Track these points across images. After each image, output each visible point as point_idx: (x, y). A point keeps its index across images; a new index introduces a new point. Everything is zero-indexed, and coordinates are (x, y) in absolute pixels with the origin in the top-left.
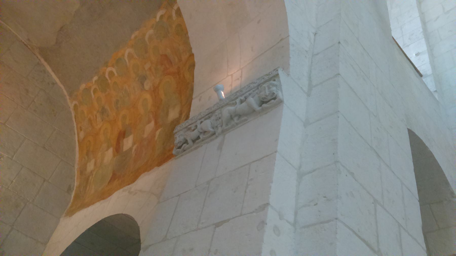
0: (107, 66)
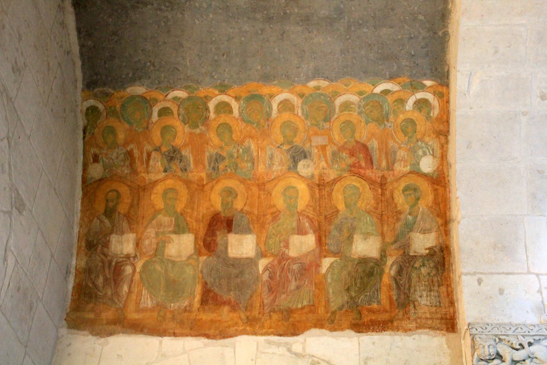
0: (222, 92)
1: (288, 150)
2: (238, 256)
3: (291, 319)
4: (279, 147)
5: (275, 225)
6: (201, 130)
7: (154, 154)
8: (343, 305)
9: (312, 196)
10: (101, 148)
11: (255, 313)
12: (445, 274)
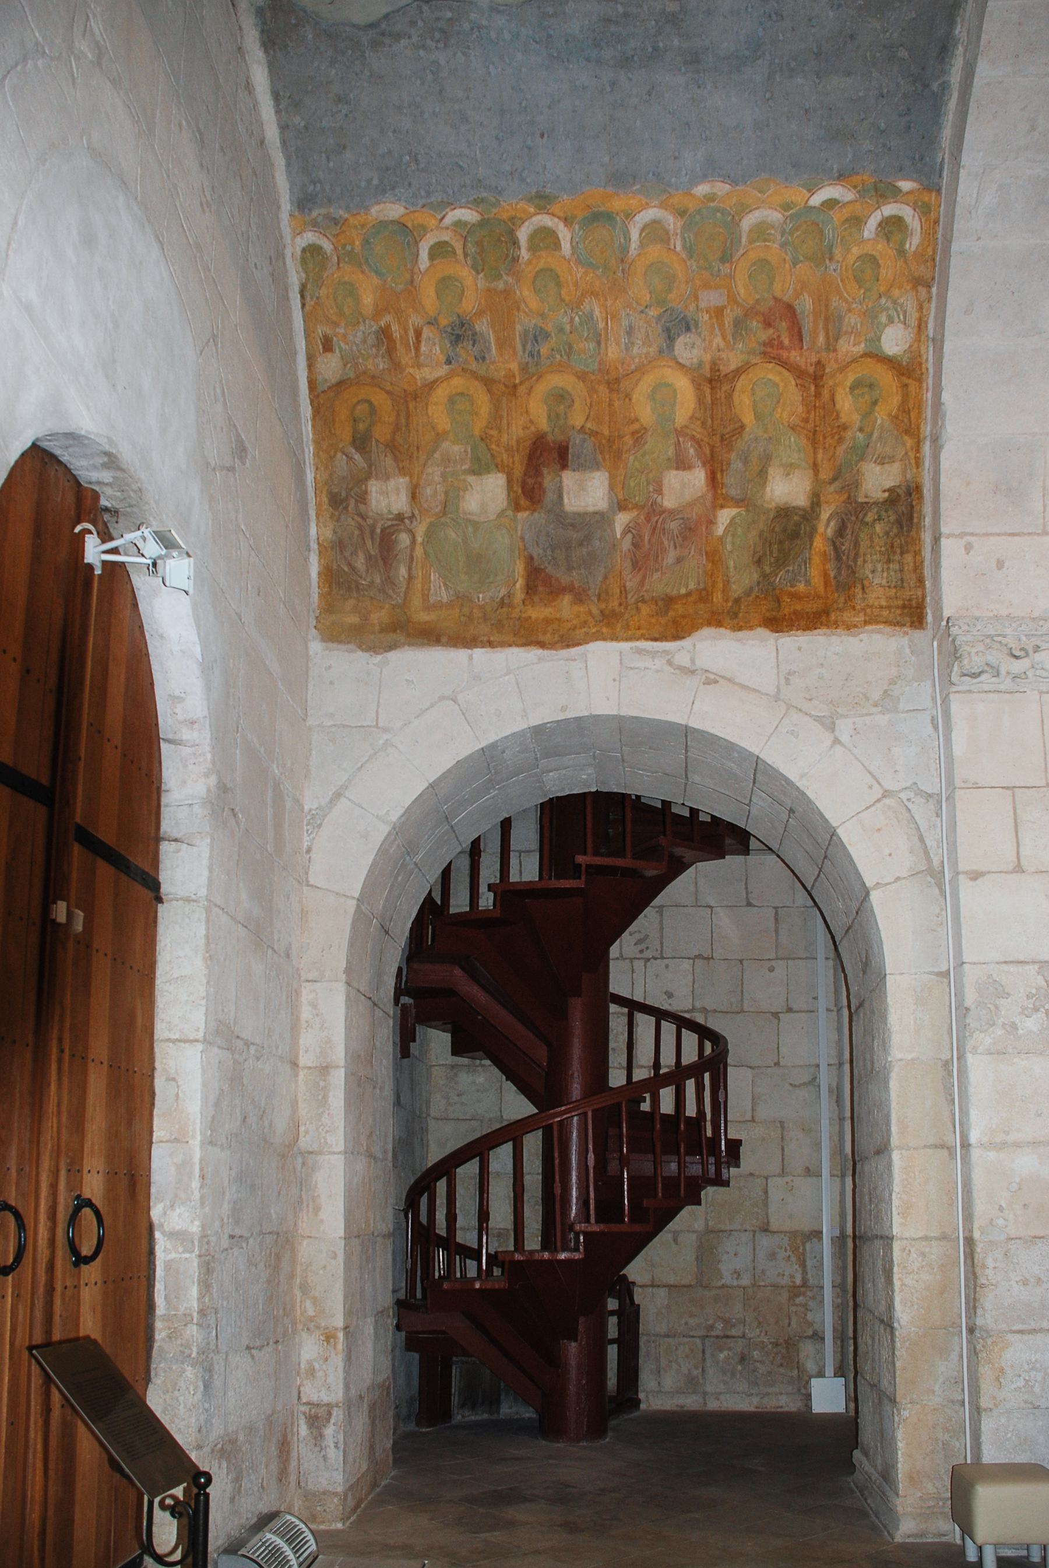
0: (541, 209)
1: (660, 317)
2: (581, 510)
3: (671, 613)
4: (642, 312)
5: (639, 455)
6: (506, 283)
7: (426, 332)
8: (751, 589)
9: (700, 400)
10: (336, 324)
11: (614, 604)
12: (913, 533)
